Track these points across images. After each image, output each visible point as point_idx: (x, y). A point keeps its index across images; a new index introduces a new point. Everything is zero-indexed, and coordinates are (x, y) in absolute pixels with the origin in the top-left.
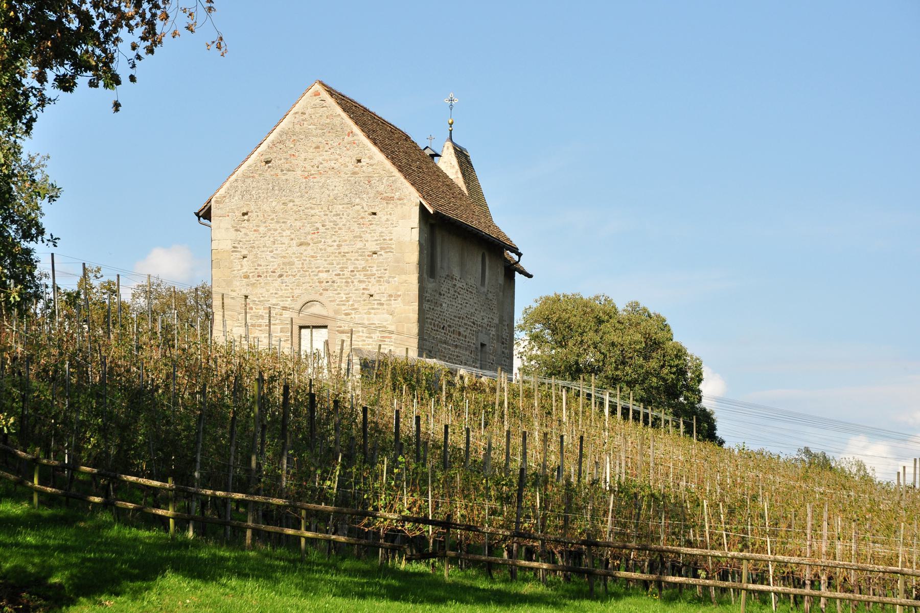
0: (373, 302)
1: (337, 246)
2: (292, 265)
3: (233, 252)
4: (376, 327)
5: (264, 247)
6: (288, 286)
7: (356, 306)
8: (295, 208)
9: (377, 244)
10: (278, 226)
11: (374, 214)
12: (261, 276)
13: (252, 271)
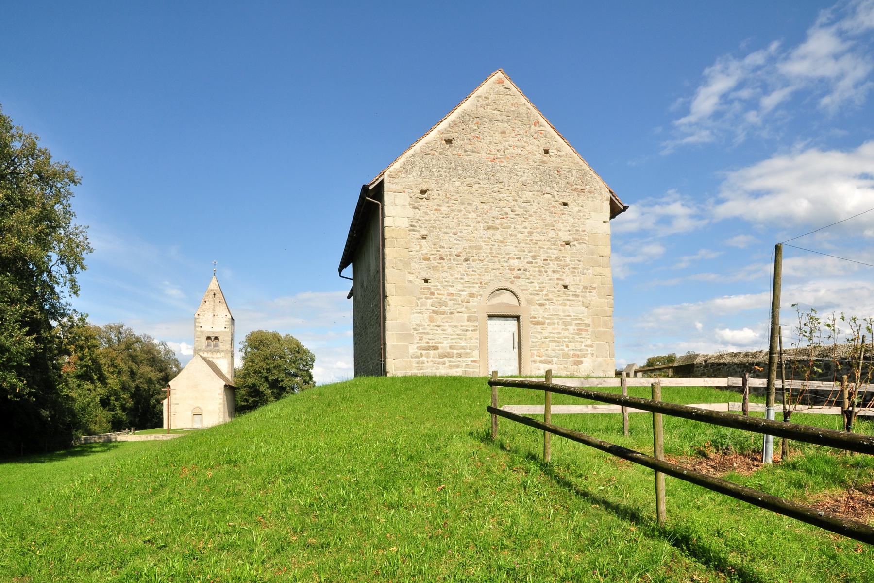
0: (569, 293)
1: (528, 233)
3: (410, 231)
4: (572, 319)
6: (475, 271)
7: (550, 296)
9: (570, 235)
10: (463, 207)
11: (565, 204)
12: (443, 259)
13: (432, 253)
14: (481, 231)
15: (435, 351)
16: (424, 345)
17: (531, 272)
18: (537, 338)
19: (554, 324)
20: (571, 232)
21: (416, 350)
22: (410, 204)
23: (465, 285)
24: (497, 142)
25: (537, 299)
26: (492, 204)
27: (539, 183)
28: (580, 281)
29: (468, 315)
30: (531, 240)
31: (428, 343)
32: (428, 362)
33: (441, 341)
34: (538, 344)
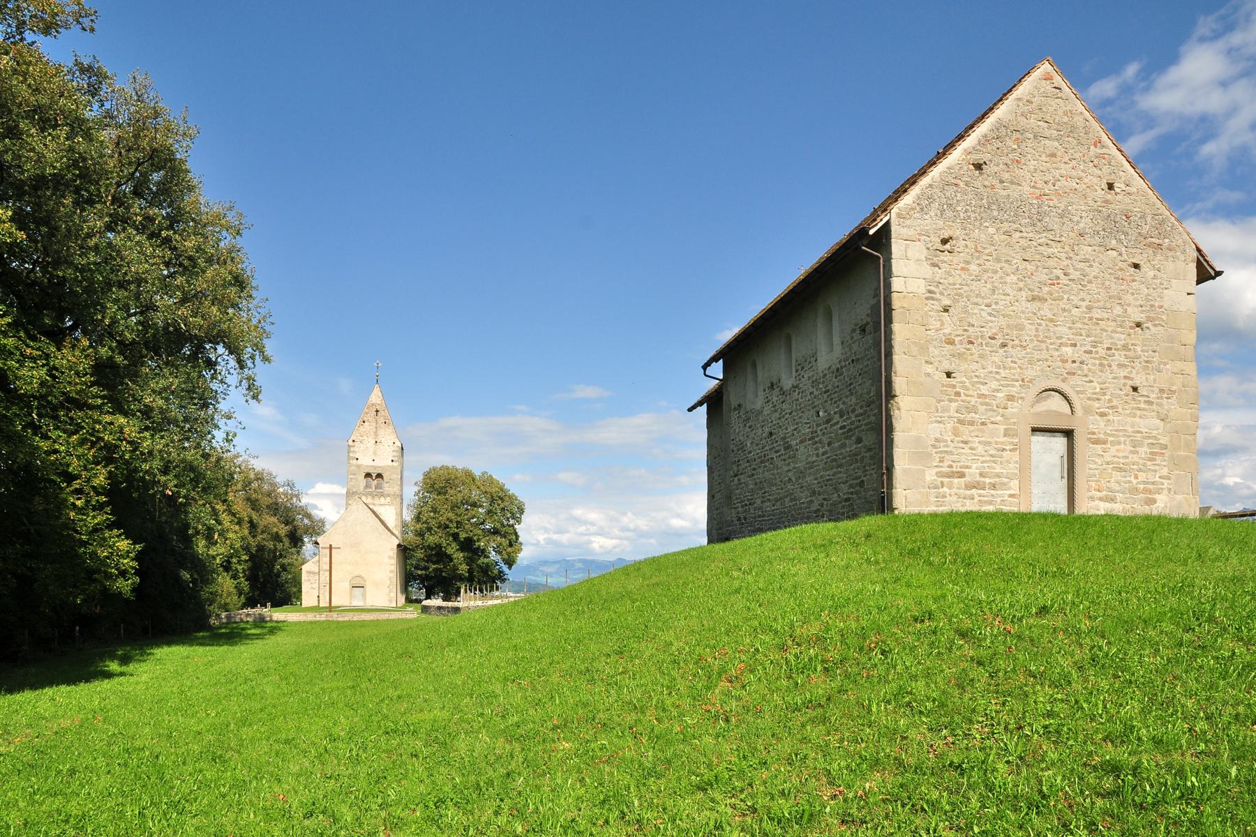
1: (1087, 307)
2: (1021, 330)
3: (927, 299)
5: (977, 296)
6: (1015, 363)
7: (1115, 403)
8: (1023, 242)
9: (1142, 312)
11: (1136, 266)
12: (973, 343)
13: (958, 333)
14: (1023, 303)
15: (960, 479)
16: (945, 469)
17: (1089, 366)
18: (1096, 463)
19: (1119, 443)
20: (1144, 308)
21: (935, 478)
22: (927, 259)
23: (1002, 383)
24: (1044, 169)
25: (1097, 405)
26: (1039, 264)
27: (1102, 233)
28: (1155, 380)
29: (1005, 427)
30: (1091, 319)
31: (951, 466)
32: (950, 495)
33: (969, 464)
34: (1097, 472)
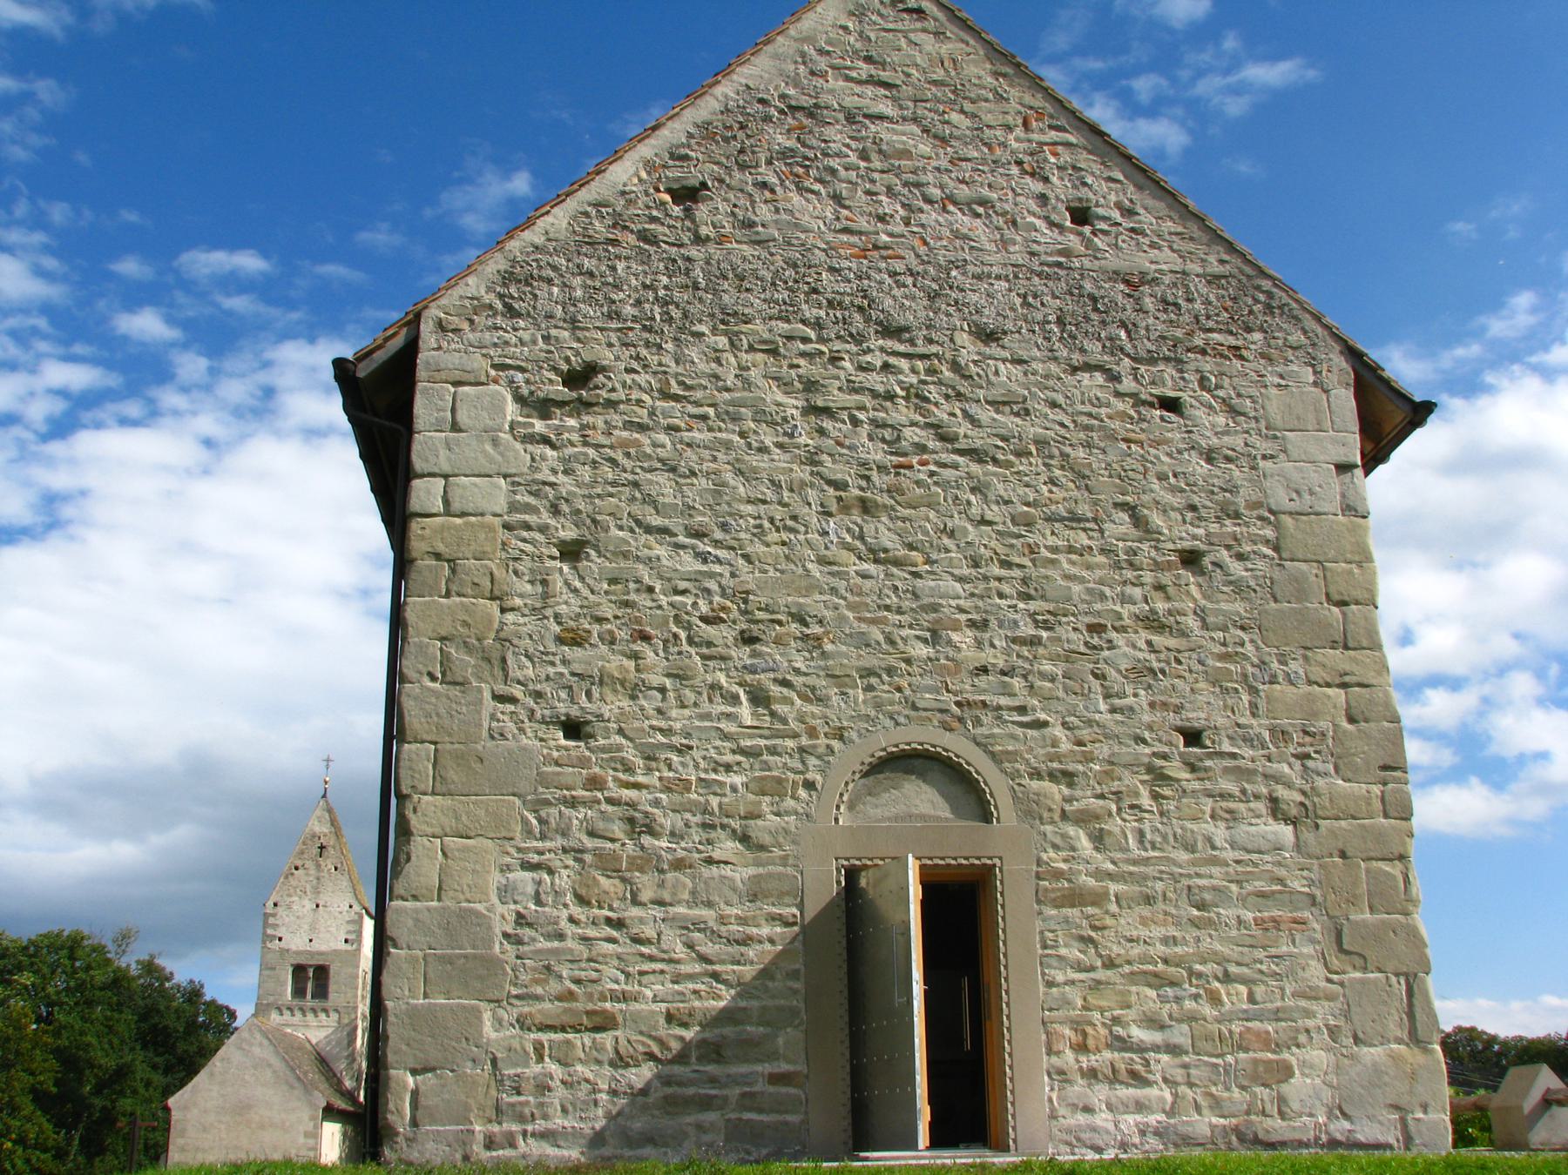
0: (1208, 763)
